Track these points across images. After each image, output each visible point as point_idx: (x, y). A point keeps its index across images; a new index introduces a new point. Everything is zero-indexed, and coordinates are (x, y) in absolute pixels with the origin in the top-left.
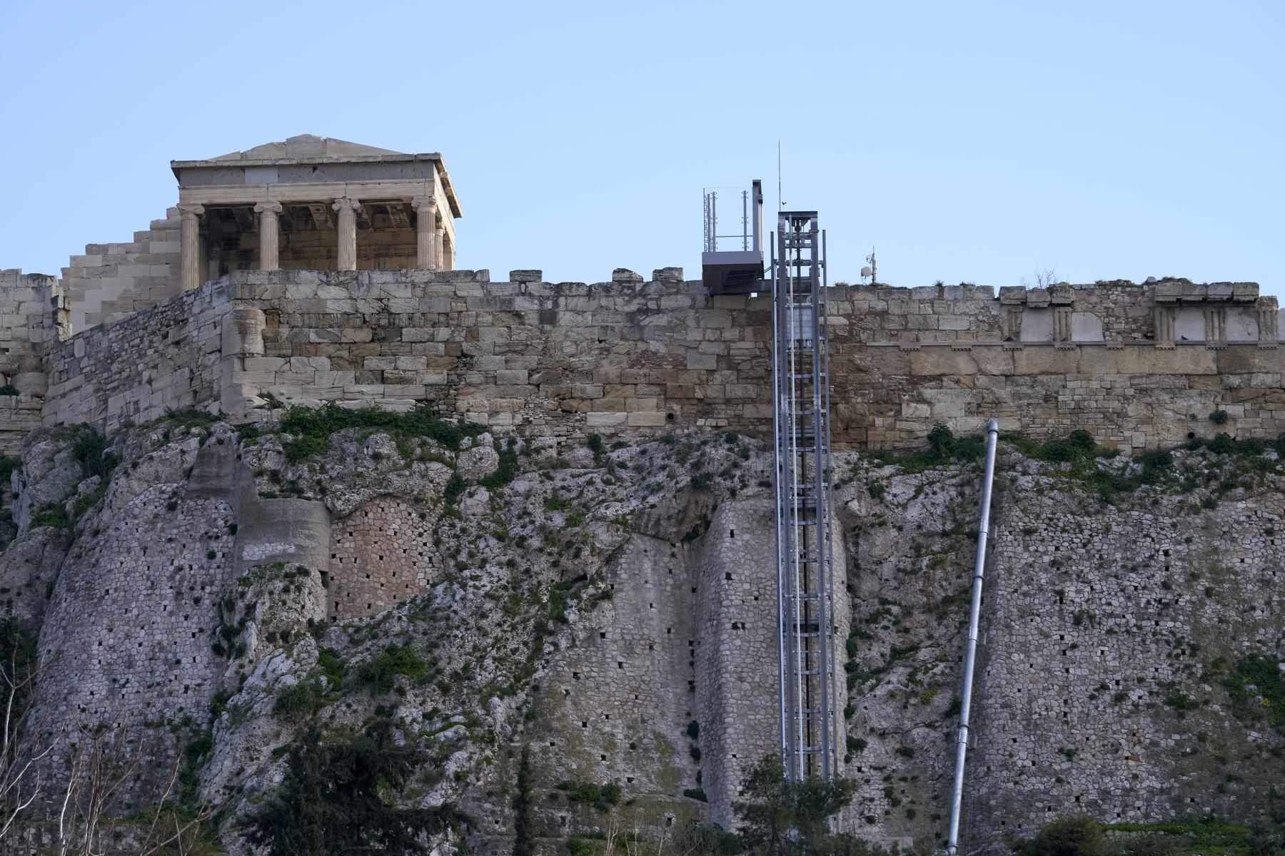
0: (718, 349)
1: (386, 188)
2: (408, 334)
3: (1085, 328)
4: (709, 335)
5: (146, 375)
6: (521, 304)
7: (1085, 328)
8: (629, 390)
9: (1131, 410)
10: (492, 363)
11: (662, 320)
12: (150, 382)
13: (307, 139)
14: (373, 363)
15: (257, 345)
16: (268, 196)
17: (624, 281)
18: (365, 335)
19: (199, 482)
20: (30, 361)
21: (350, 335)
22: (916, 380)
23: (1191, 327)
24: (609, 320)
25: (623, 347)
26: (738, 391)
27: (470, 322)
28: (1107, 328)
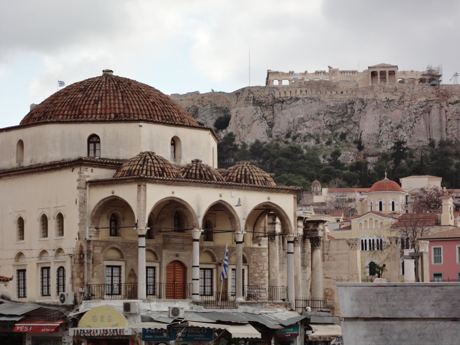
1: (392, 69)
10: (407, 93)
13: (383, 64)
14: (394, 94)
15: (382, 92)
16: (379, 70)
19: (377, 106)
21: (392, 90)
22: (453, 95)
25: (421, 92)
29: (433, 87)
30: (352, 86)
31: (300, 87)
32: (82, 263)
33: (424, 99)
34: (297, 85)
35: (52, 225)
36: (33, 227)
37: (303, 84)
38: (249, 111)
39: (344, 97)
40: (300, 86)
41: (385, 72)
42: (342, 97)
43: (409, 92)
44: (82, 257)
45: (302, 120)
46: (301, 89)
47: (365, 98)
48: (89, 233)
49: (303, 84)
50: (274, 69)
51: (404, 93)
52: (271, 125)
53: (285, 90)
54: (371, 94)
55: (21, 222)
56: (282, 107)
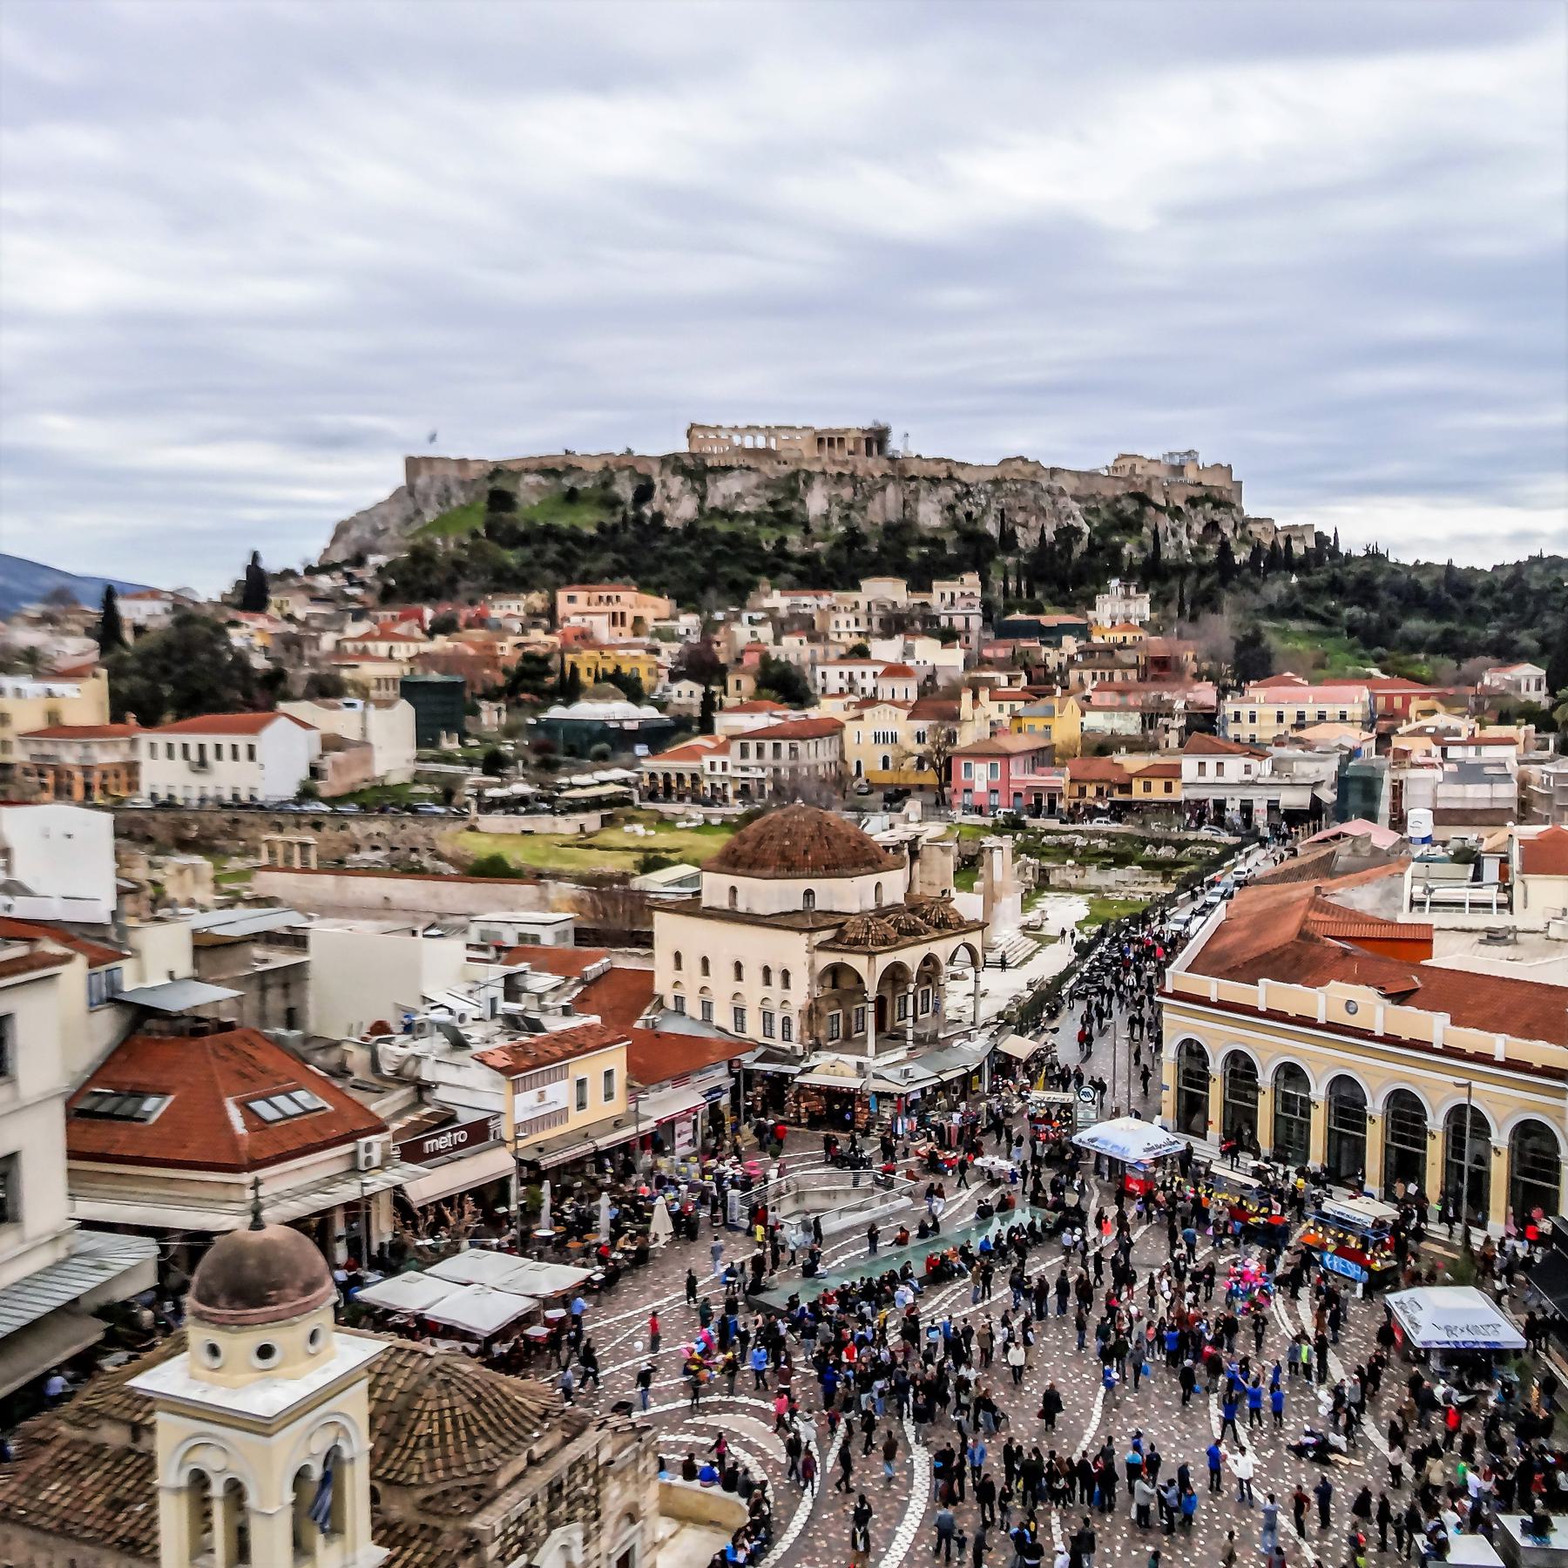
16: (826, 437)
30: (796, 454)
32: (810, 1018)
35: (776, 978)
36: (753, 974)
38: (676, 483)
44: (812, 1013)
45: (738, 495)
47: (811, 469)
48: (817, 992)
50: (698, 422)
52: (703, 498)
55: (738, 967)
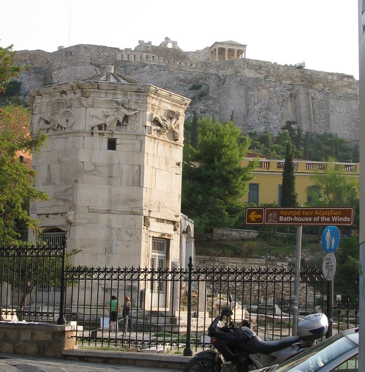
0: (296, 75)
2: (263, 68)
3: (335, 78)
4: (296, 73)
5: (226, 69)
6: (275, 66)
7: (335, 78)
8: (287, 78)
9: (340, 88)
10: (272, 73)
11: (291, 70)
12: (227, 70)
14: (259, 71)
15: (246, 68)
16: (227, 47)
17: (286, 65)
18: (258, 68)
20: (205, 64)
21: (256, 67)
23: (346, 79)
24: (285, 70)
25: (287, 73)
26: (299, 80)
27: (270, 68)
28: (337, 78)
29: (299, 69)
31: (147, 53)
33: (289, 82)
34: (143, 49)
37: (150, 49)
39: (193, 70)
40: (147, 50)
41: (233, 51)
42: (191, 70)
43: (274, 72)
46: (147, 54)
47: (220, 73)
49: (150, 49)
51: (269, 73)
53: (129, 53)
54: (230, 70)
56: (125, 71)
